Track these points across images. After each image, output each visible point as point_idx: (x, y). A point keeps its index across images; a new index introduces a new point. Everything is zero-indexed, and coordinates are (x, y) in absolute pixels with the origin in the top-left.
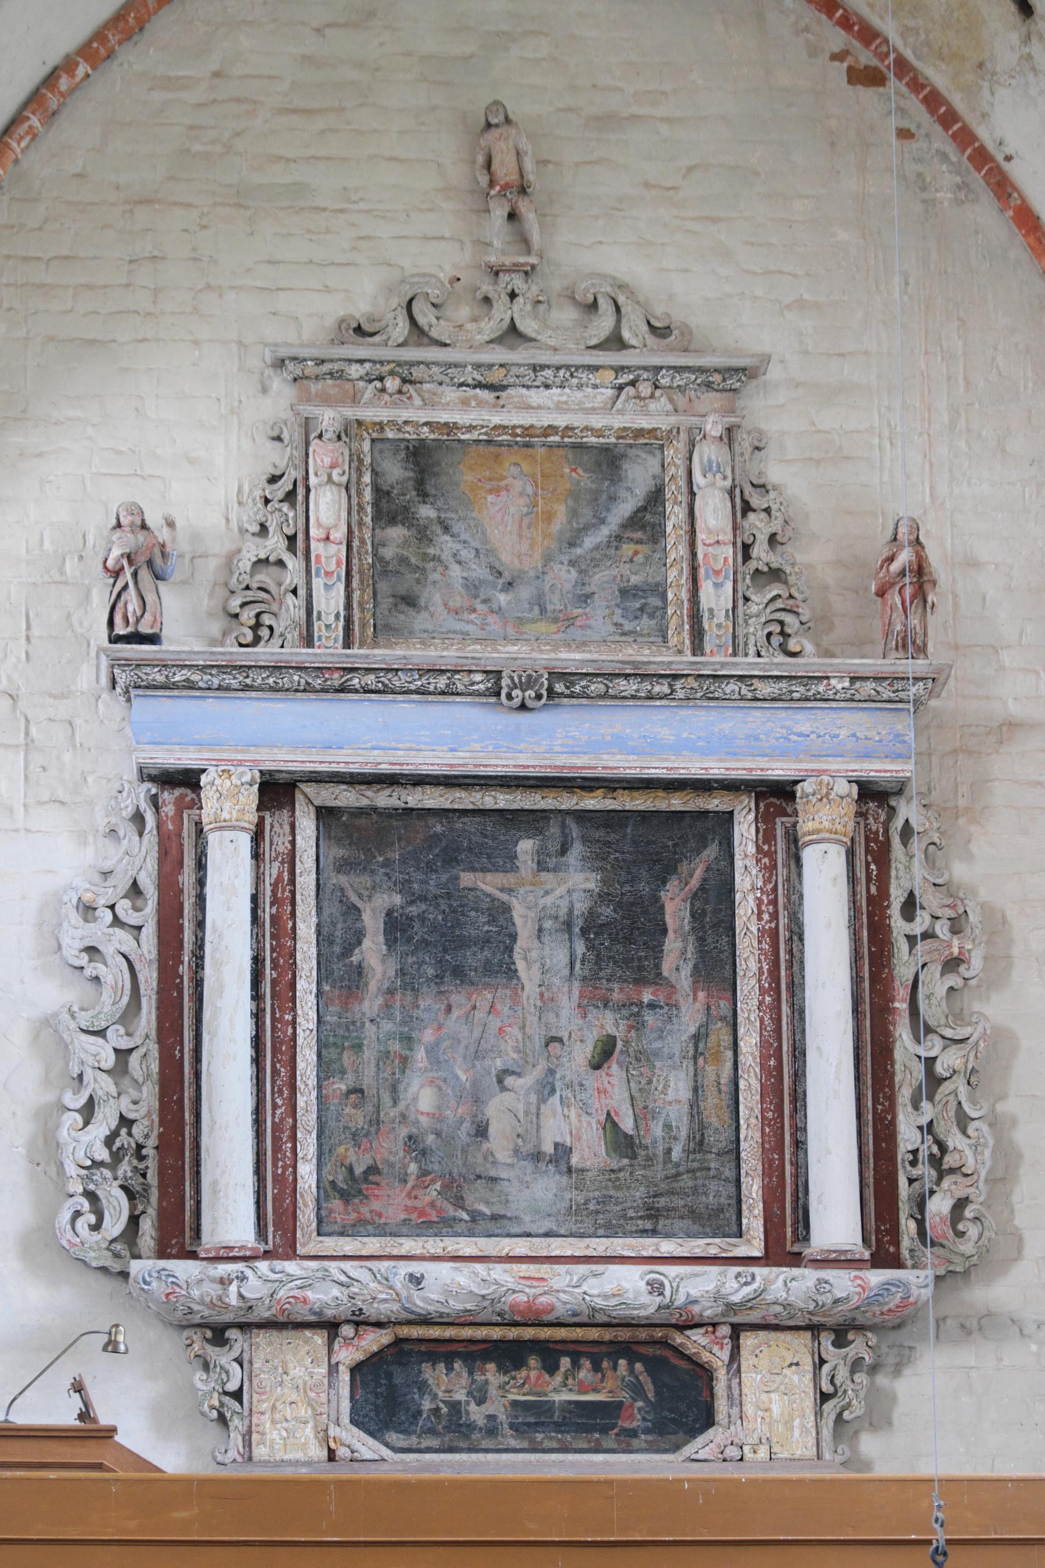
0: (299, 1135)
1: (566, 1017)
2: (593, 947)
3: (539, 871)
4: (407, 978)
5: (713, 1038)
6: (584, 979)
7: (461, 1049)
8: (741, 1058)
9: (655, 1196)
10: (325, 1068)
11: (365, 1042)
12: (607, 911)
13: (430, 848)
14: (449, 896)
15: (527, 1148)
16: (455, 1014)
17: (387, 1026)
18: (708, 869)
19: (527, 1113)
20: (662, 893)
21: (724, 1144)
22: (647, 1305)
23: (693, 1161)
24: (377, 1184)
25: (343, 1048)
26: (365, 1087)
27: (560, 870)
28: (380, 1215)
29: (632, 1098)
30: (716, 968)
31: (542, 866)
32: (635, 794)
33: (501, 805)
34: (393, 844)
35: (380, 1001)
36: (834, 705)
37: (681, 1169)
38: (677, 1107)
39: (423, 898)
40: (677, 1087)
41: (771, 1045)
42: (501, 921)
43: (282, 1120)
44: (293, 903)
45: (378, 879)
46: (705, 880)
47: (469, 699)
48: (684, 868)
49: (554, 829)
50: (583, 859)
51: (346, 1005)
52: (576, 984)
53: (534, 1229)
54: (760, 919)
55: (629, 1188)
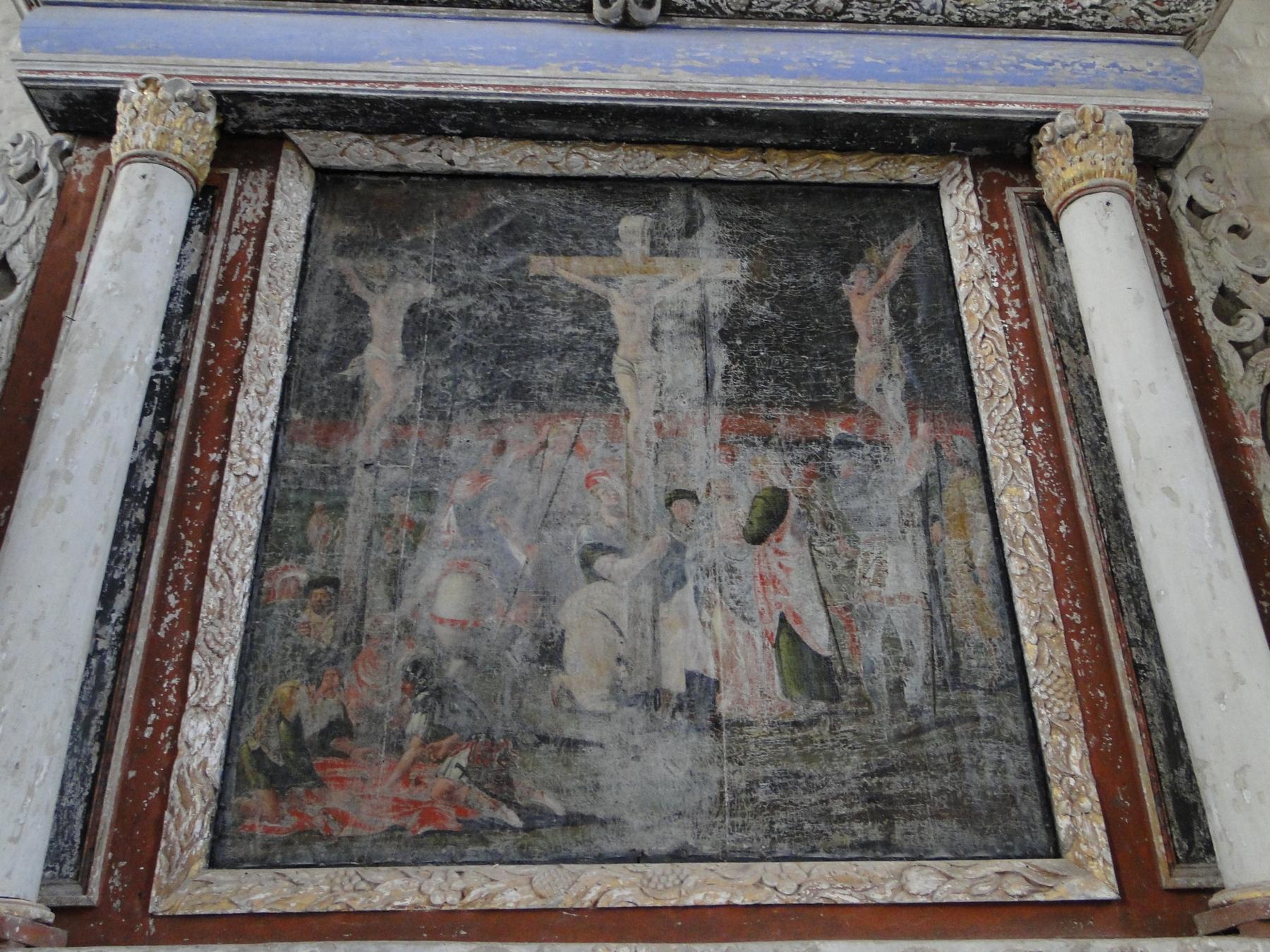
0: (196, 660)
1: (701, 459)
2: (742, 358)
3: (652, 255)
4: (434, 401)
5: (951, 493)
6: (729, 403)
7: (519, 511)
8: (1005, 523)
9: (882, 773)
10: (271, 543)
11: (352, 500)
12: (761, 310)
13: (486, 225)
14: (511, 287)
15: (638, 682)
16: (511, 455)
17: (393, 474)
18: (910, 256)
19: (635, 619)
20: (844, 287)
21: (997, 671)
23: (945, 704)
24: (345, 756)
25: (312, 510)
26: (341, 576)
27: (686, 254)
28: (343, 819)
29: (823, 592)
30: (943, 388)
31: (656, 249)
32: (795, 155)
33: (596, 169)
34: (429, 220)
35: (385, 434)
36: (1076, 35)
37: (926, 719)
38: (904, 607)
39: (468, 289)
40: (898, 574)
41: (1056, 500)
42: (594, 319)
43: (171, 632)
44: (254, 287)
45: (400, 264)
46: (907, 270)
47: (546, 15)
48: (874, 254)
49: (675, 204)
50: (720, 241)
51: (325, 442)
52: (717, 412)
53: (649, 843)
54: (1004, 316)
55: (830, 758)
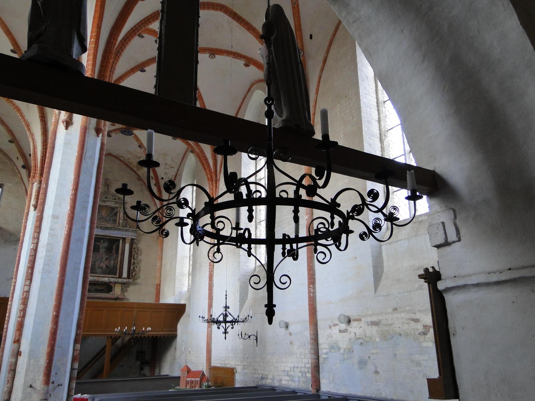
22: (108, 281)
30: (117, 252)
40: (112, 262)
